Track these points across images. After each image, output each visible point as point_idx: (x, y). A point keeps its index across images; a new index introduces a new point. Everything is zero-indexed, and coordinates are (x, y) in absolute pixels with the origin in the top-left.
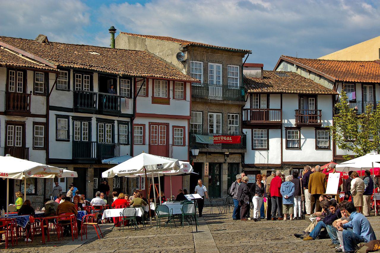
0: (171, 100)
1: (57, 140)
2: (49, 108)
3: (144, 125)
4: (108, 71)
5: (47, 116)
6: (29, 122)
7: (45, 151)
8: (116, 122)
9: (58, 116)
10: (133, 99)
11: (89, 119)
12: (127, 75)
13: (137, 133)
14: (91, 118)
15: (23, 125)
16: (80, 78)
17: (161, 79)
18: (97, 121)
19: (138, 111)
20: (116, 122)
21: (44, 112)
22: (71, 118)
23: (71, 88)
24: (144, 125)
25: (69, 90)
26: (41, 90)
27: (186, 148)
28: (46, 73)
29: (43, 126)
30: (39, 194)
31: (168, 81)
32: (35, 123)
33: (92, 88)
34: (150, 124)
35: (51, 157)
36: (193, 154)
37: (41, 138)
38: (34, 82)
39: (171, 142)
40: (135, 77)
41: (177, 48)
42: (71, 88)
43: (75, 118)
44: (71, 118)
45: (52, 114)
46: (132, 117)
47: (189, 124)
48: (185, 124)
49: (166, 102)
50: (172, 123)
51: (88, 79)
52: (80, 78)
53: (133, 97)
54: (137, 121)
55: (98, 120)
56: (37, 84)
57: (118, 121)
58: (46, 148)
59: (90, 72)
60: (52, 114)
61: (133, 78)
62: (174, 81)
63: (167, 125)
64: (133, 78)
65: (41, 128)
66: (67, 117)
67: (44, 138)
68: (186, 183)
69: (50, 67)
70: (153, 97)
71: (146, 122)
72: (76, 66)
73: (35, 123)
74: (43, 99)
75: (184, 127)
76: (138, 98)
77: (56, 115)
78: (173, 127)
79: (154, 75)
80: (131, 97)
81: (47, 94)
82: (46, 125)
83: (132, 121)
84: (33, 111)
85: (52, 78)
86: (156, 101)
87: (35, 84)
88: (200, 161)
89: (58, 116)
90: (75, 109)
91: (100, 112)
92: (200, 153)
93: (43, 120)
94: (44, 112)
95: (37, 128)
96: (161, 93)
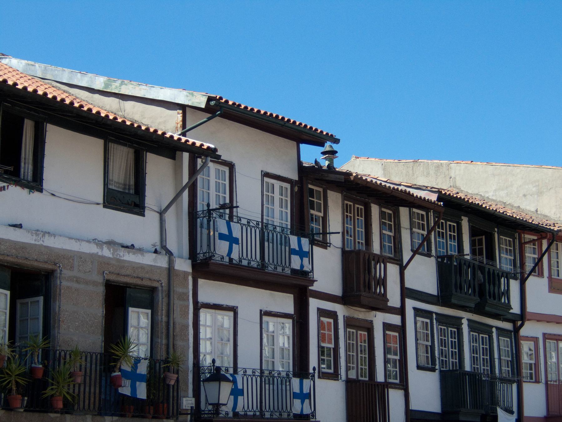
5: (401, 311)
8: (494, 330)
9: (418, 312)
14: (461, 318)
19: (531, 308)
20: (494, 330)
42: (433, 252)
57: (498, 328)
58: (404, 385)
60: (410, 304)
70: (550, 277)
82: (402, 329)
83: (517, 330)
89: (418, 312)
93: (395, 320)
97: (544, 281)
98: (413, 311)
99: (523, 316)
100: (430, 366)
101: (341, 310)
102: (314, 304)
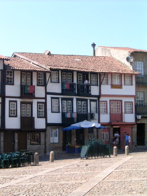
0: (123, 86)
1: (52, 112)
2: (47, 93)
3: (106, 102)
4: (81, 70)
5: (45, 98)
6: (35, 102)
7: (45, 119)
9: (52, 98)
10: (99, 86)
11: (72, 100)
12: (94, 72)
13: (102, 107)
14: (73, 98)
15: (31, 103)
16: (65, 75)
17: (116, 73)
18: (76, 100)
19: (102, 93)
21: (44, 96)
22: (60, 99)
23: (60, 81)
24: (106, 102)
25: (59, 82)
26: (42, 83)
27: (133, 115)
28: (45, 73)
29: (43, 104)
30: (42, 144)
31: (121, 74)
32: (38, 103)
33: (73, 81)
34: (110, 101)
35: (48, 122)
36: (138, 118)
37: (42, 112)
38: (37, 78)
39: (123, 111)
40: (100, 73)
41: (127, 54)
42: (60, 81)
43: (62, 99)
44: (60, 99)
45: (49, 97)
46: (99, 97)
47: (135, 100)
48: (132, 100)
49: (120, 87)
50: (124, 100)
51: (70, 75)
52: (65, 75)
53: (99, 85)
54: (102, 99)
55: (77, 100)
56: (39, 80)
58: (45, 117)
59: (72, 72)
60: (49, 97)
61: (98, 74)
62: (124, 74)
63: (121, 101)
64: (98, 74)
65: (42, 106)
66: (58, 98)
67: (44, 111)
68: (134, 136)
69: (46, 69)
71: (108, 99)
72: (62, 68)
73: (38, 103)
74: (43, 88)
75: (132, 102)
76: (102, 86)
77: (51, 97)
78: (125, 102)
79: (111, 71)
80: (97, 85)
81: (45, 85)
82: (45, 103)
84: (36, 96)
85: (48, 75)
86: (113, 86)
87: (38, 80)
88: (143, 122)
89: (52, 98)
90: (62, 94)
91: (78, 95)
92: (142, 117)
93: (43, 101)
94: (44, 96)
95: (40, 106)
96: (116, 82)
97: (110, 86)
98: (51, 98)
99: (99, 97)
100: (58, 111)
101: (19, 101)
102: (7, 100)
